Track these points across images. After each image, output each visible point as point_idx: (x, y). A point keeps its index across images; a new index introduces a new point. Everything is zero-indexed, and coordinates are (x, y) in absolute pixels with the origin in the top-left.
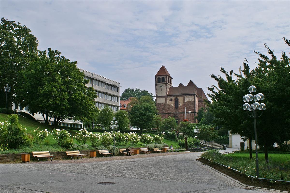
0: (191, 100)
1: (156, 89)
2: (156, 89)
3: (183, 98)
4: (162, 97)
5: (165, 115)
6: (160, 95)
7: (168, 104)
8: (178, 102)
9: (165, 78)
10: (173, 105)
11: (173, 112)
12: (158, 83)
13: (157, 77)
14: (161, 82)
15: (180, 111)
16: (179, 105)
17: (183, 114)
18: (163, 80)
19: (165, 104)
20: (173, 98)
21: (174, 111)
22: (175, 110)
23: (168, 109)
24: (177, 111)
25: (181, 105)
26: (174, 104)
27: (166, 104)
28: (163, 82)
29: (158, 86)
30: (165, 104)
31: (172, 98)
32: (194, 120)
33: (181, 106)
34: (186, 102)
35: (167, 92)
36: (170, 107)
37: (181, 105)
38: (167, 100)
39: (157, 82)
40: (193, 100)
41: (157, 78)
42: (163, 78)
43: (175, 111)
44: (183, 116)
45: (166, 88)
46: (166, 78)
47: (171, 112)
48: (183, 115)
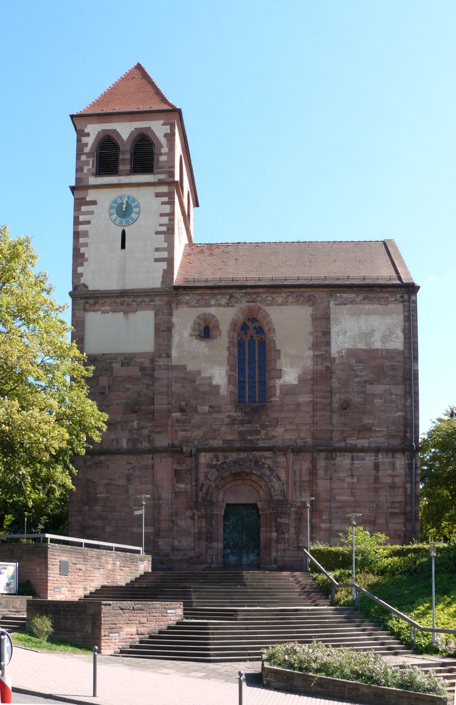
0: (385, 339)
1: (81, 228)
2: (81, 228)
3: (315, 319)
4: (124, 300)
5: (147, 460)
6: (114, 286)
7: (175, 362)
8: (263, 344)
9: (163, 141)
10: (219, 375)
11: (217, 443)
12: (93, 181)
13: (94, 130)
14: (128, 167)
15: (279, 431)
16: (279, 382)
17: (314, 461)
18: (144, 156)
19: (152, 361)
20: (226, 315)
21: (228, 434)
22: (242, 423)
23: (177, 415)
24: (258, 433)
25: (290, 376)
26: (232, 368)
27: (161, 362)
28: (136, 170)
29: (94, 203)
30: (152, 361)
31: (212, 311)
32: (401, 520)
33: (290, 391)
34: (334, 350)
35: (170, 261)
37: (290, 376)
38: (169, 330)
39: (86, 169)
40: (397, 343)
41: (90, 141)
43: (240, 433)
44: (306, 478)
45: (165, 220)
46: (170, 137)
48: (313, 472)
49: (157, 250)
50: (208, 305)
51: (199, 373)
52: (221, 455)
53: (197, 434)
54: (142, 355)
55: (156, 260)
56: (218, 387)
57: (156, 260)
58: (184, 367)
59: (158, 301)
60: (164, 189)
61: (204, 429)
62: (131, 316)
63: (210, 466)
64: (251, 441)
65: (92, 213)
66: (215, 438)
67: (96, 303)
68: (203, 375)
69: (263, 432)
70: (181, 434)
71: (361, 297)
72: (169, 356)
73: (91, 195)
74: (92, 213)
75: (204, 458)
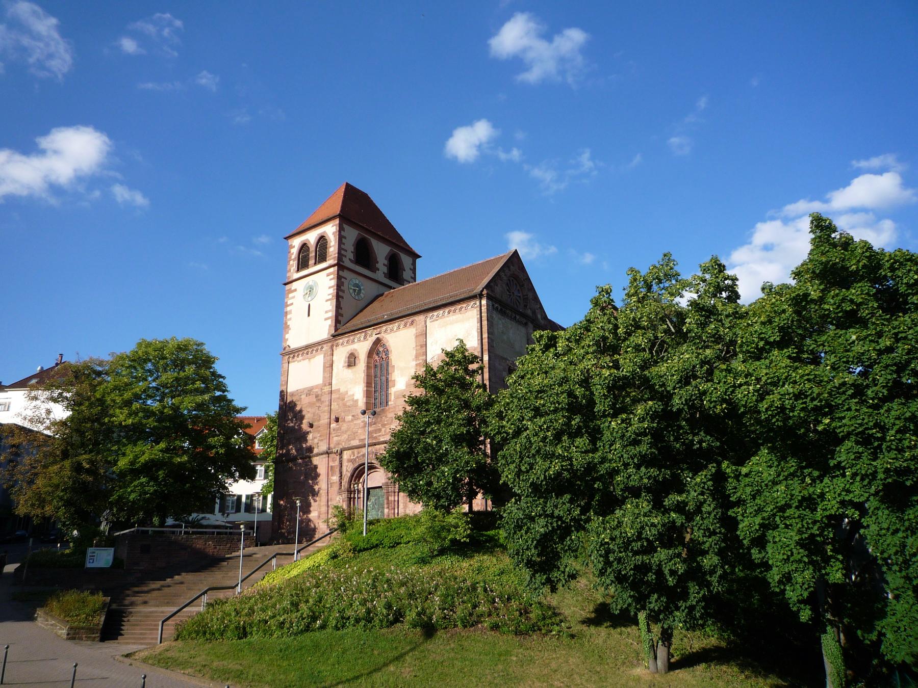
11: (356, 443)
13: (297, 242)
22: (370, 424)
23: (333, 425)
24: (380, 430)
29: (295, 290)
36: (345, 405)
42: (322, 240)
47: (349, 440)
49: (326, 312)
50: (353, 342)
51: (347, 392)
52: (356, 450)
53: (345, 436)
54: (317, 386)
55: (326, 319)
56: (357, 401)
57: (326, 319)
58: (338, 390)
59: (326, 347)
60: (332, 270)
61: (349, 433)
62: (312, 360)
63: (350, 461)
64: (376, 438)
65: (293, 297)
66: (354, 439)
67: (294, 357)
68: (350, 393)
69: (383, 429)
70: (336, 439)
71: (447, 310)
72: (331, 384)
73: (294, 285)
74: (293, 297)
75: (346, 455)
